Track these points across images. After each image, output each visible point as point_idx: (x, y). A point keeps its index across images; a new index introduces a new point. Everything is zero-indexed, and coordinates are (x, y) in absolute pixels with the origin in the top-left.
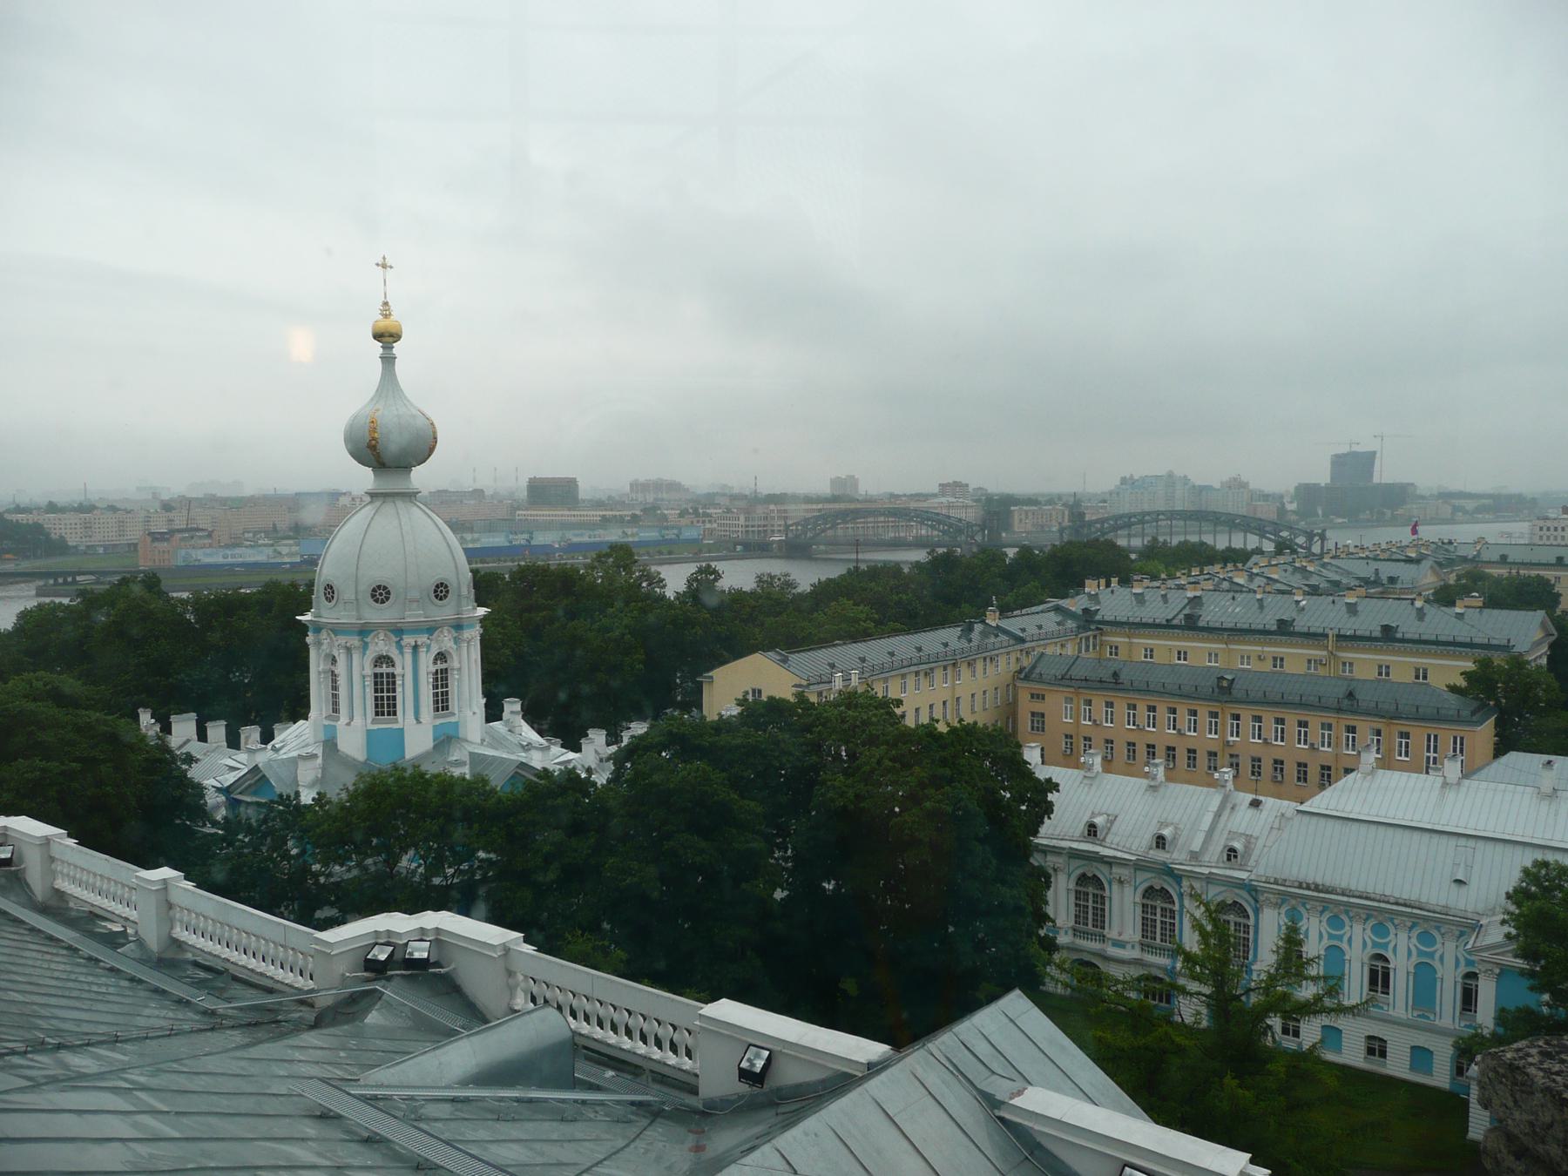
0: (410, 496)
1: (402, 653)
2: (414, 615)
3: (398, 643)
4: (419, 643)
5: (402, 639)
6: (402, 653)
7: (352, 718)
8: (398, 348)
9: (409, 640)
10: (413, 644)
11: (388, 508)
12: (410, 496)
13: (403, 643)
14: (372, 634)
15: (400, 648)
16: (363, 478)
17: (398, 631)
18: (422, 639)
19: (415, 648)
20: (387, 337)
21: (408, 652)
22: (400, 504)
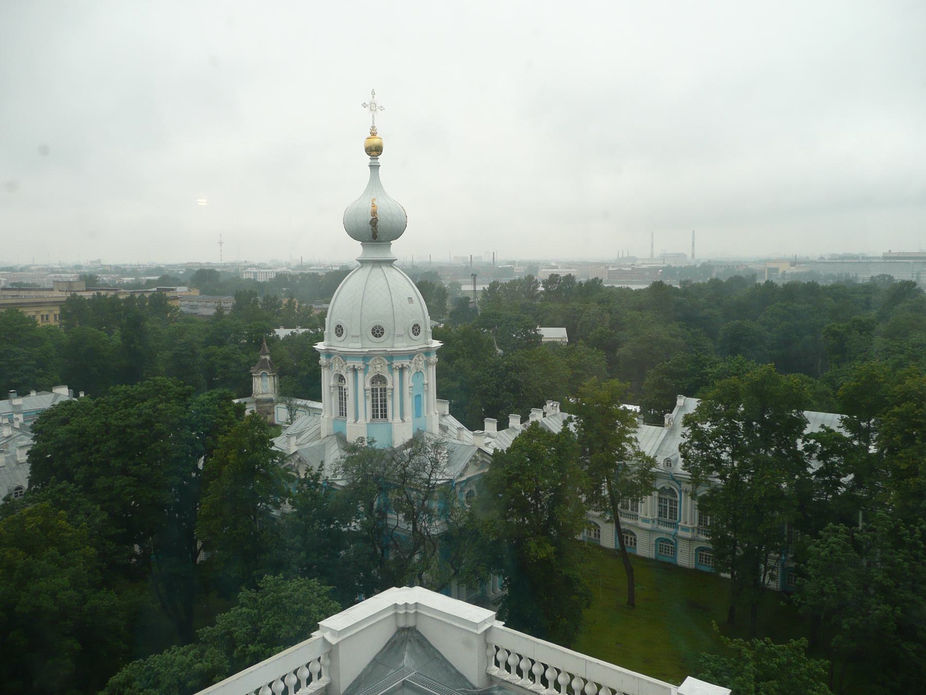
0: (390, 262)
2: (401, 346)
3: (390, 366)
4: (405, 366)
7: (356, 419)
8: (381, 158)
9: (397, 363)
10: (400, 367)
11: (377, 271)
12: (390, 262)
13: (394, 366)
14: (372, 360)
15: (391, 369)
16: (354, 250)
17: (390, 357)
18: (406, 363)
19: (402, 370)
20: (374, 151)
21: (397, 374)
22: (385, 269)
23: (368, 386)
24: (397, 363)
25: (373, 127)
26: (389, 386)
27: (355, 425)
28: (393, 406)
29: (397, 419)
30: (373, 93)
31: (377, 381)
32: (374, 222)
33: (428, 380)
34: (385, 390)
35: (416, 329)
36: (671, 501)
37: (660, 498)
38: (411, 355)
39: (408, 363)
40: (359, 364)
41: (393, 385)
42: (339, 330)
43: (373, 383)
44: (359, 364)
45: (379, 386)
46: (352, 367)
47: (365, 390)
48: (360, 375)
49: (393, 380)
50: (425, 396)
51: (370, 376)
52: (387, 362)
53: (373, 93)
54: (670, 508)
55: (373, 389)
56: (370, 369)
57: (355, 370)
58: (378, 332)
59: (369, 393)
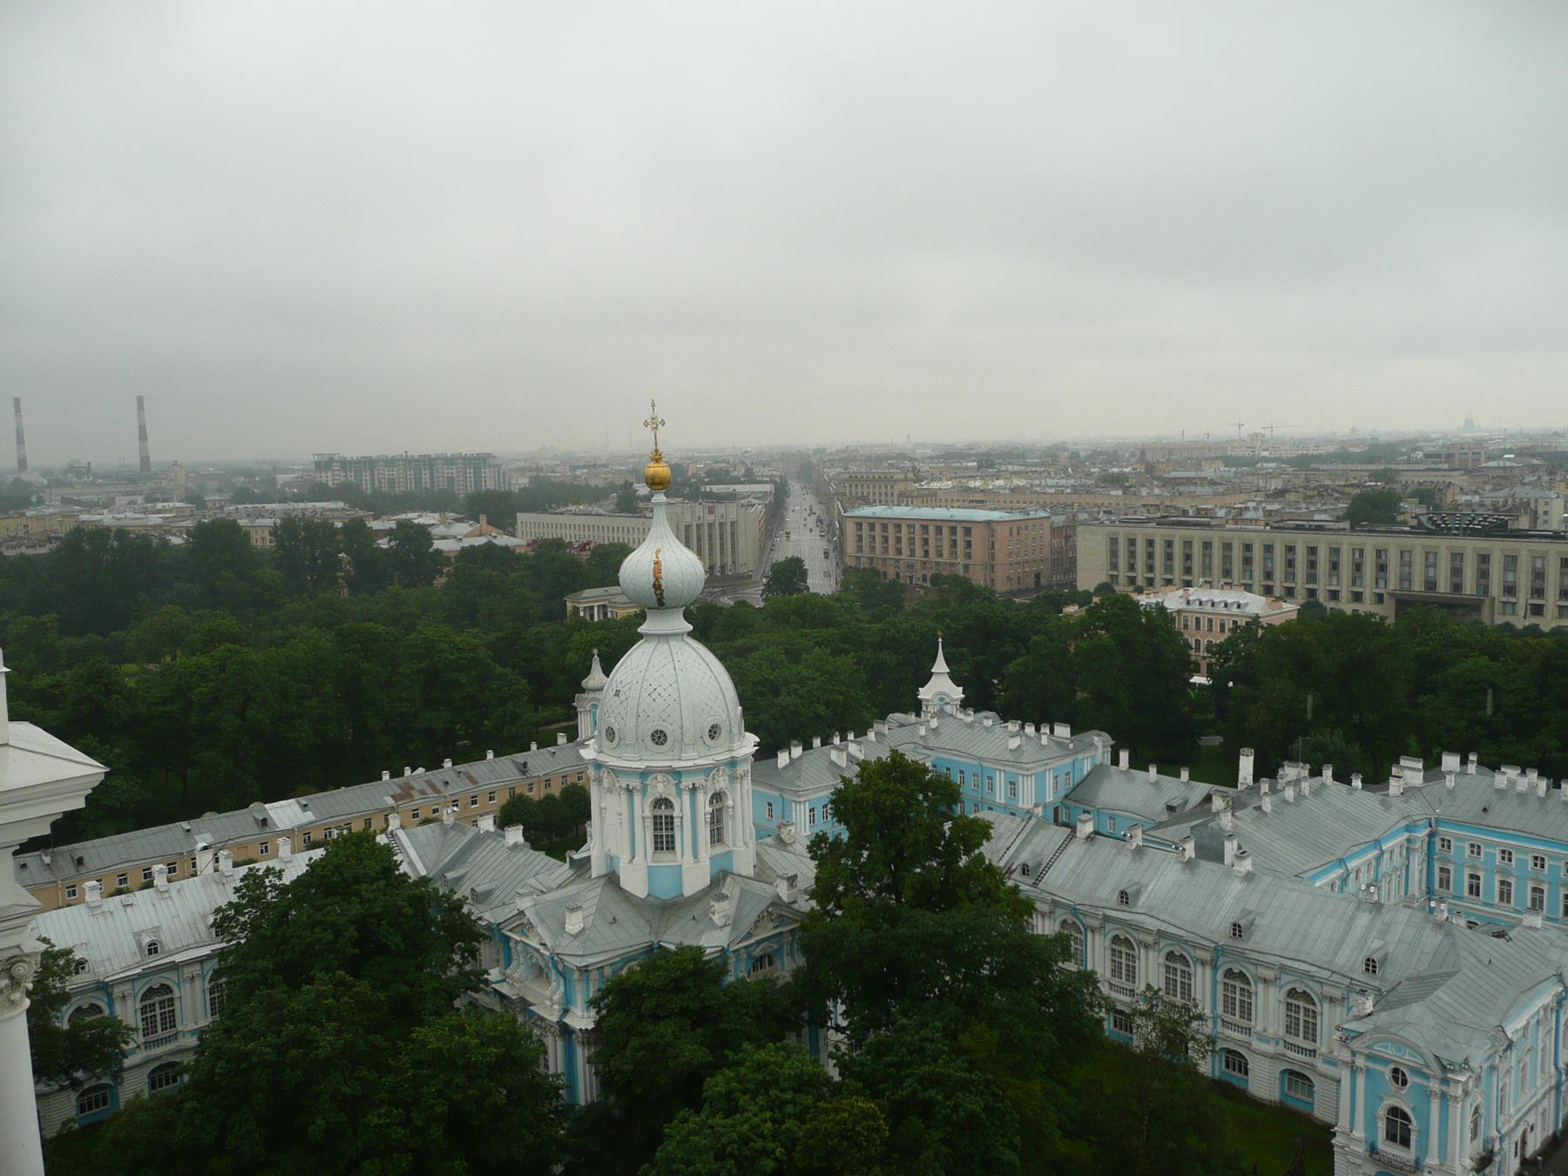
1: (680, 795)
3: (677, 785)
5: (680, 782)
6: (680, 795)
9: (687, 782)
10: (691, 787)
13: (682, 786)
15: (679, 792)
17: (677, 774)
18: (699, 780)
19: (694, 790)
21: (686, 797)
23: (648, 813)
24: (687, 782)
25: (656, 451)
26: (676, 813)
27: (628, 865)
28: (683, 836)
29: (689, 857)
30: (653, 405)
31: (661, 805)
32: (657, 586)
33: (734, 800)
34: (672, 817)
35: (714, 732)
36: (1128, 954)
37: (1112, 949)
38: (706, 771)
39: (703, 782)
40: (635, 783)
41: (681, 811)
42: (611, 733)
43: (655, 807)
44: (635, 783)
45: (663, 812)
46: (624, 786)
47: (643, 818)
48: (637, 798)
49: (682, 809)
50: (730, 824)
51: (650, 799)
52: (673, 782)
53: (653, 405)
54: (1127, 965)
55: (655, 817)
56: (649, 789)
57: (629, 791)
58: (659, 737)
59: (650, 823)
